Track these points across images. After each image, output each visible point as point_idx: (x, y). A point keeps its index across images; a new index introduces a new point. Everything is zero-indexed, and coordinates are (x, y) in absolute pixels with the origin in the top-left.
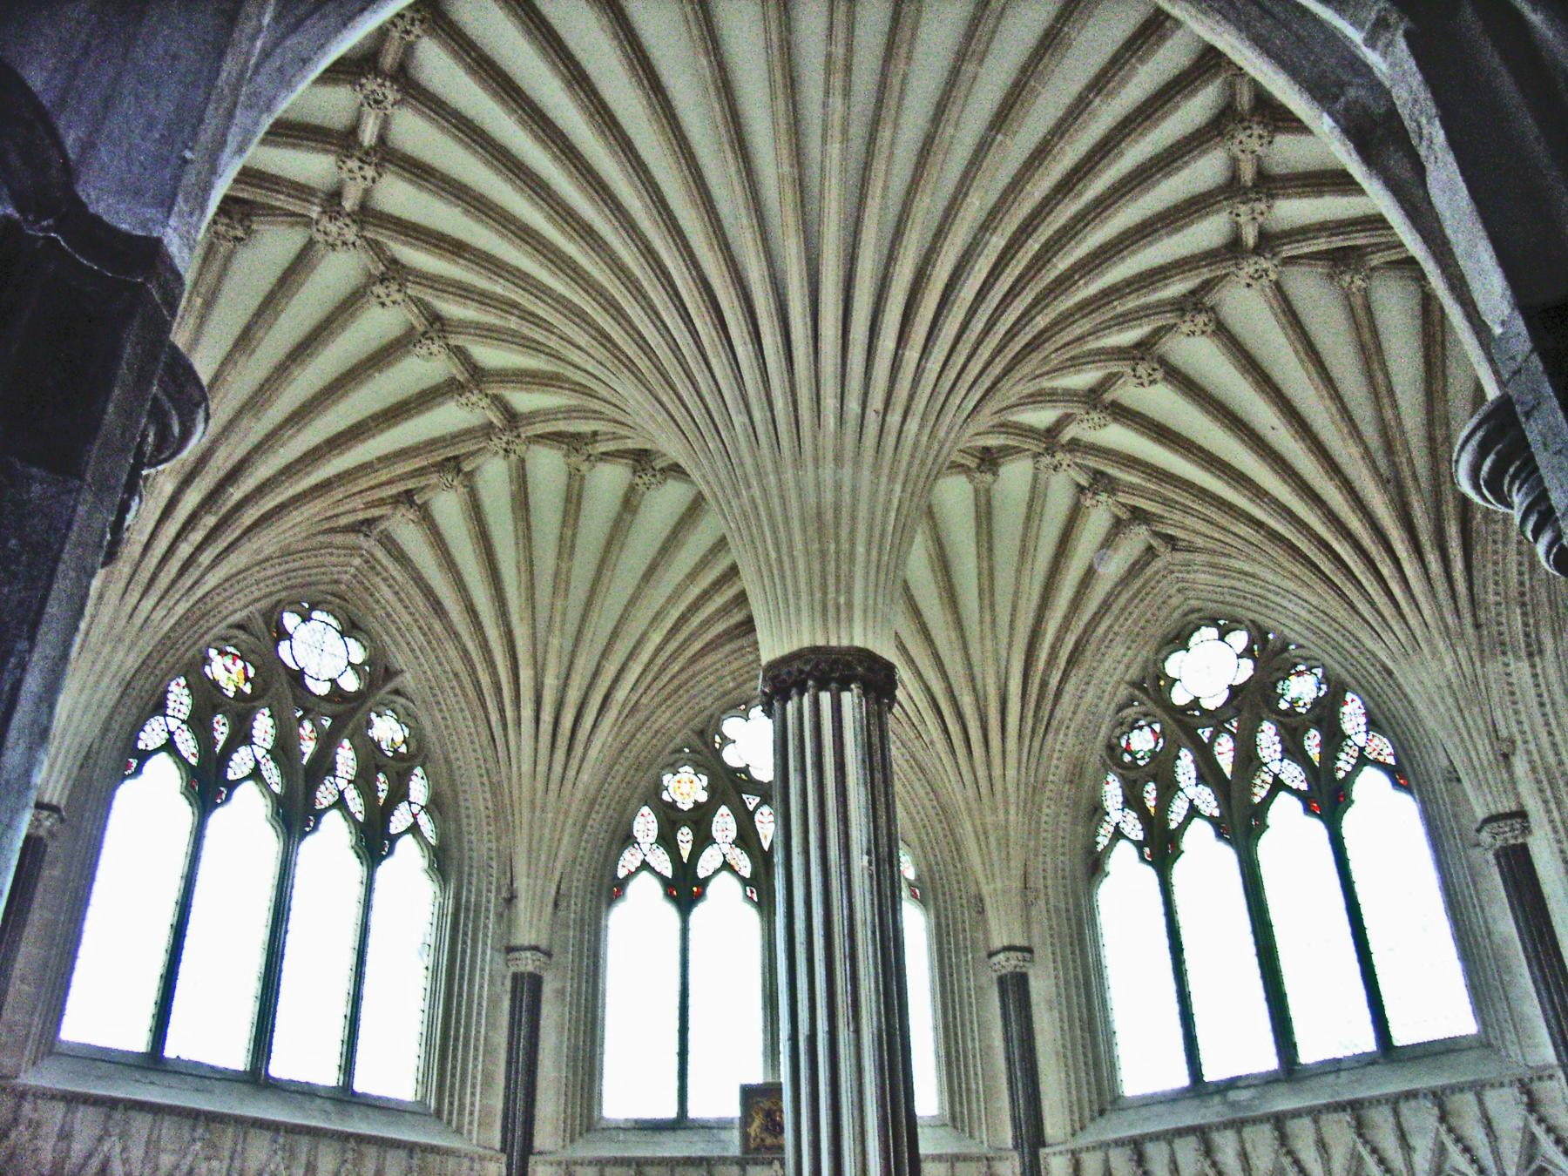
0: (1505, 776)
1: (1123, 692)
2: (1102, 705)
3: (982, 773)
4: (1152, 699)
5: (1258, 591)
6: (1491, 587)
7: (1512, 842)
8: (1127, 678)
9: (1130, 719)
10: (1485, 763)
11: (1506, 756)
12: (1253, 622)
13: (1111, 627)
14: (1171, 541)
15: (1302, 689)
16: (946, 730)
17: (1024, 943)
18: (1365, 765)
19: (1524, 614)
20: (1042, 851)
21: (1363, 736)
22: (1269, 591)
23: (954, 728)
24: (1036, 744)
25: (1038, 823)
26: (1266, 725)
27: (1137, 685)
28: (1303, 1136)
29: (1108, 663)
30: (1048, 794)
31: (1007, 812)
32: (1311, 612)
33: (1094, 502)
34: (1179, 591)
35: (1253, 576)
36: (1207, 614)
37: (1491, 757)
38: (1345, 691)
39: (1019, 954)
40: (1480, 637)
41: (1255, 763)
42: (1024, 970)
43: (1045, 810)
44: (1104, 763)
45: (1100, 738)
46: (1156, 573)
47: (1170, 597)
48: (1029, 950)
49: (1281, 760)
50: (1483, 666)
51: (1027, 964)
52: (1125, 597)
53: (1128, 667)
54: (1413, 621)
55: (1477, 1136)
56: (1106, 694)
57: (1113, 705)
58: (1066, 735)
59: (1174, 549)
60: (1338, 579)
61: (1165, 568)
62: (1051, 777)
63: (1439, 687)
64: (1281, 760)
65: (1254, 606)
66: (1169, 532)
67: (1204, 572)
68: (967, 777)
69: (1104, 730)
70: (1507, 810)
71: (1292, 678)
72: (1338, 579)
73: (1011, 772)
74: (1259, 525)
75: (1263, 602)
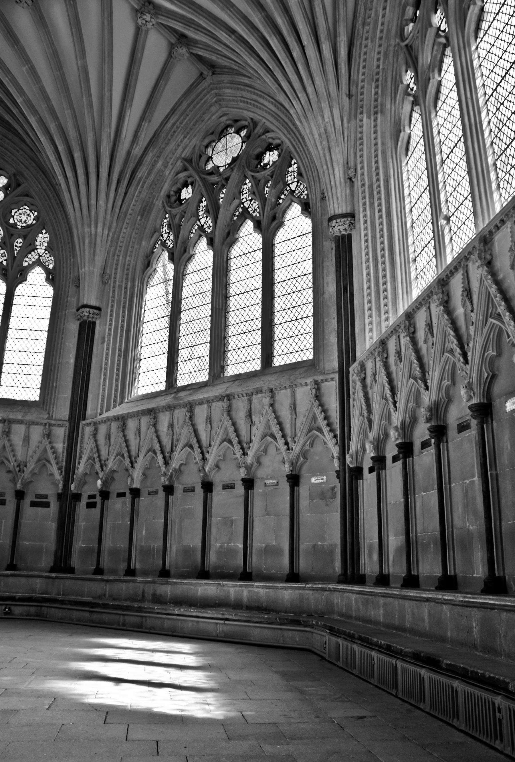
0: (348, 191)
1: (179, 164)
2: (167, 173)
3: (84, 202)
4: (192, 167)
5: (255, 97)
6: (361, 71)
7: (344, 233)
8: (183, 156)
9: (181, 181)
10: (338, 182)
11: (350, 179)
12: (252, 119)
13: (175, 123)
14: (212, 67)
15: (271, 157)
16: (66, 177)
17: (97, 305)
18: (292, 201)
19: (377, 87)
20: (117, 253)
21: (295, 184)
22: (257, 95)
23: (70, 174)
24: (122, 190)
25: (119, 237)
26: (247, 181)
27: (189, 161)
28: (201, 413)
29: (172, 146)
30: (127, 221)
31: (96, 227)
32: (275, 106)
33: (144, 22)
34: (216, 102)
35: (250, 86)
36: (230, 117)
37: (342, 180)
38: (292, 159)
39: (91, 310)
40: (350, 104)
41: (236, 202)
42: (94, 320)
43: (124, 230)
44: (164, 206)
45: (163, 191)
46: (204, 89)
47: (211, 106)
48: (99, 309)
49: (251, 200)
50: (349, 122)
51: (96, 316)
52: (185, 104)
53: (184, 149)
54: (310, 89)
55: (286, 414)
56: (169, 164)
57: (173, 171)
58: (142, 187)
59: (213, 74)
60: (272, 64)
61: (209, 86)
62: (130, 211)
63: (320, 135)
64: (251, 200)
65: (253, 109)
66: (200, 53)
67: (228, 88)
68: (76, 204)
69: (166, 187)
70: (344, 212)
71: (268, 153)
72: (272, 64)
73: (102, 203)
74: (232, 32)
75: (256, 104)
